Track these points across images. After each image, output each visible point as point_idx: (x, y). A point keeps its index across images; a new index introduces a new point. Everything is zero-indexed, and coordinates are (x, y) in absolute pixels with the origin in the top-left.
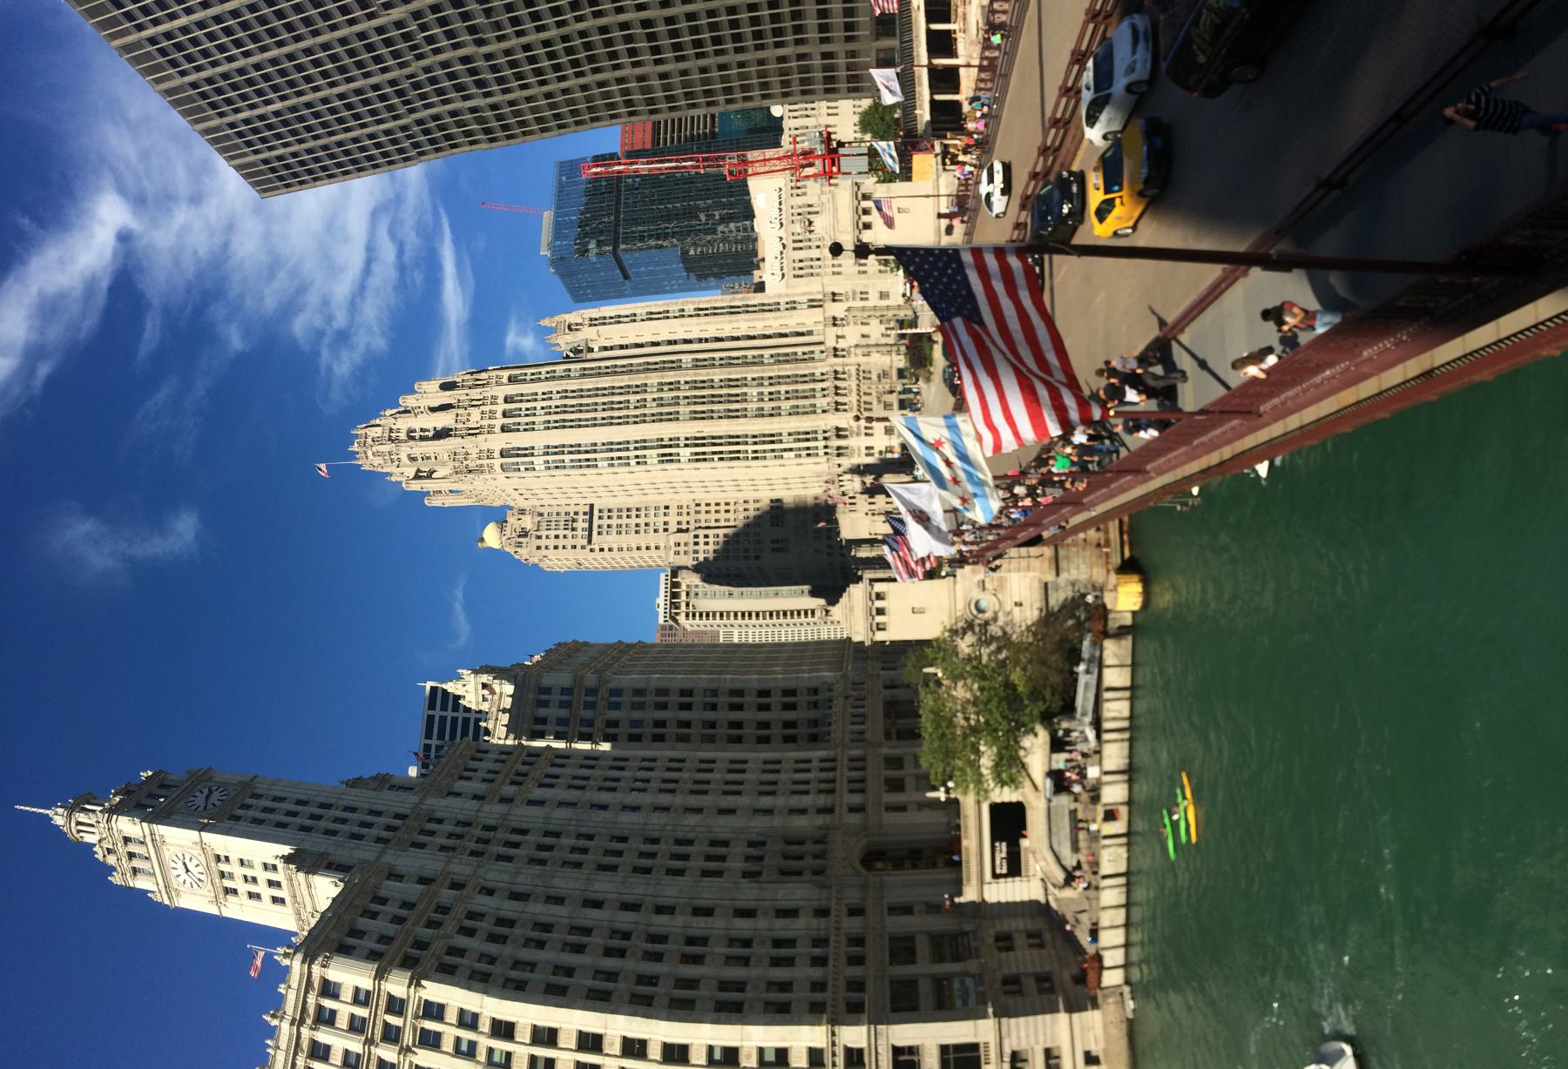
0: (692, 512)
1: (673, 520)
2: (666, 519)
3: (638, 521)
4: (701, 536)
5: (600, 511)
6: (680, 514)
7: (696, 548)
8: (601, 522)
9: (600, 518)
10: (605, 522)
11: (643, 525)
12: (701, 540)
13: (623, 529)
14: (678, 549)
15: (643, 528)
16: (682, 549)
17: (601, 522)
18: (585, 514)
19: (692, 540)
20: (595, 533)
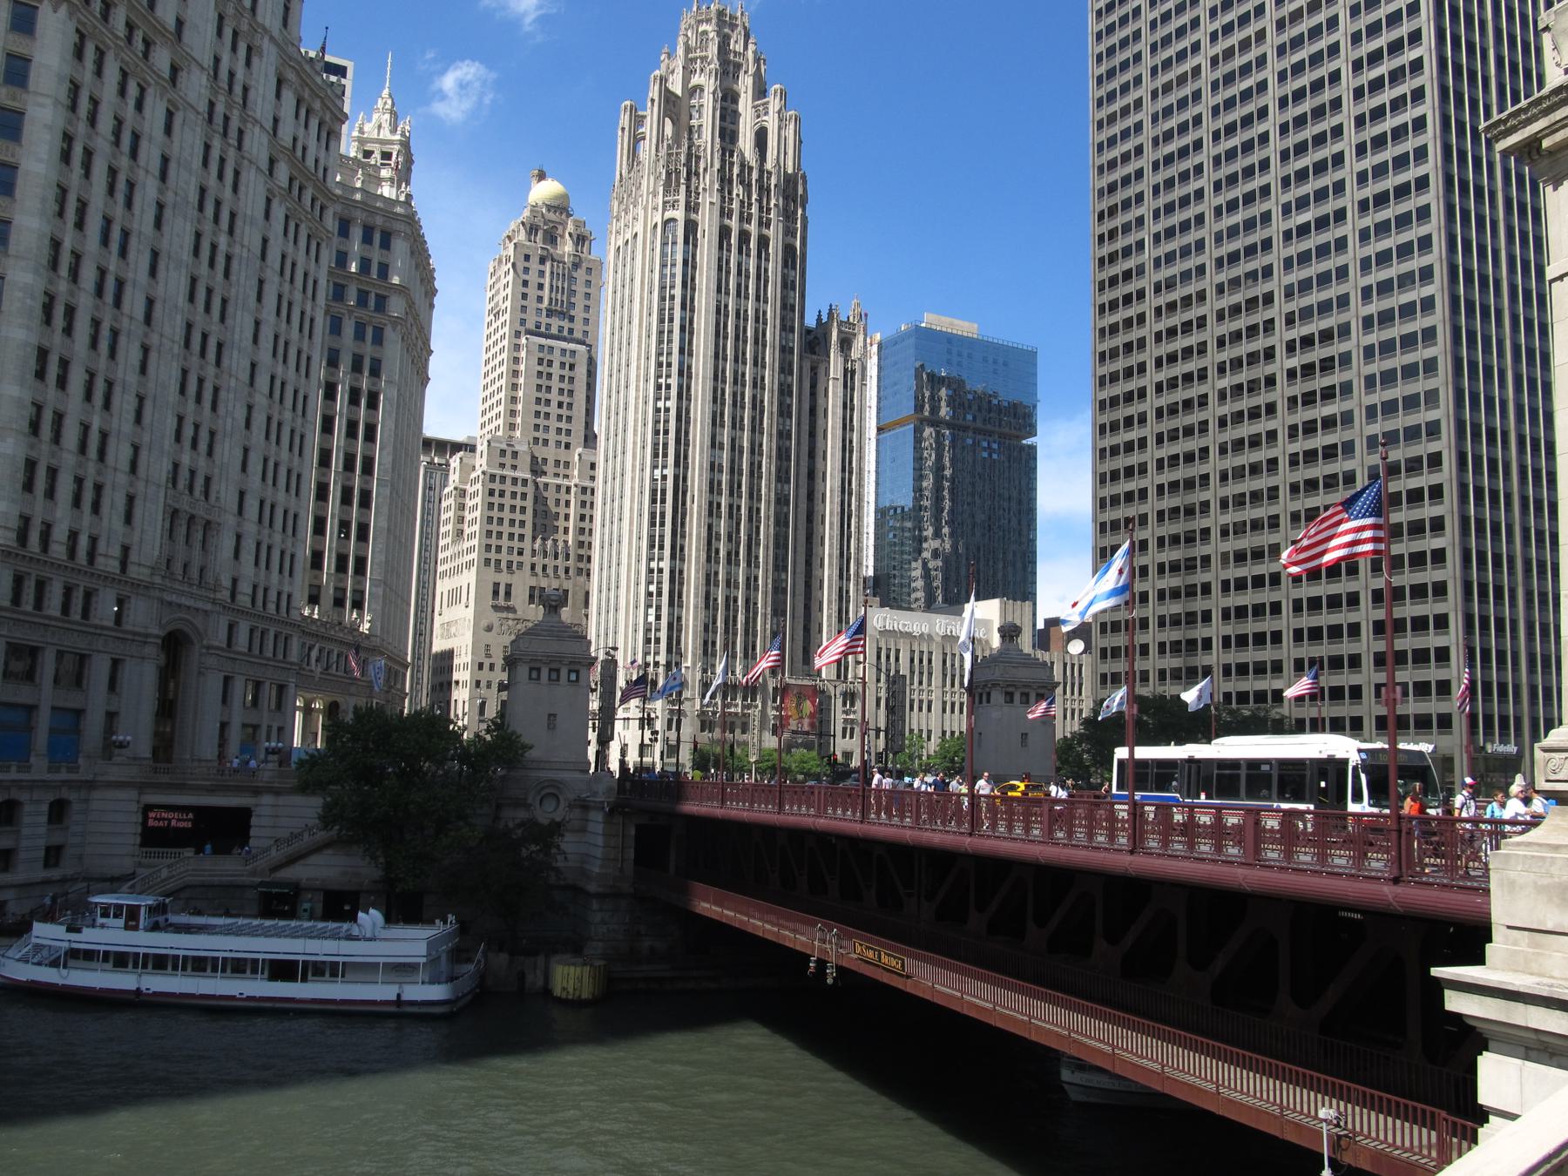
0: (559, 481)
1: (550, 453)
2: (552, 443)
3: (554, 404)
4: (524, 490)
5: (573, 352)
6: (557, 463)
7: (509, 481)
8: (557, 353)
9: (564, 351)
10: (557, 358)
11: (547, 409)
12: (519, 489)
13: (544, 382)
14: (509, 454)
15: (543, 409)
16: (508, 460)
17: (557, 353)
18: (571, 331)
19: (517, 474)
20: (543, 341)
